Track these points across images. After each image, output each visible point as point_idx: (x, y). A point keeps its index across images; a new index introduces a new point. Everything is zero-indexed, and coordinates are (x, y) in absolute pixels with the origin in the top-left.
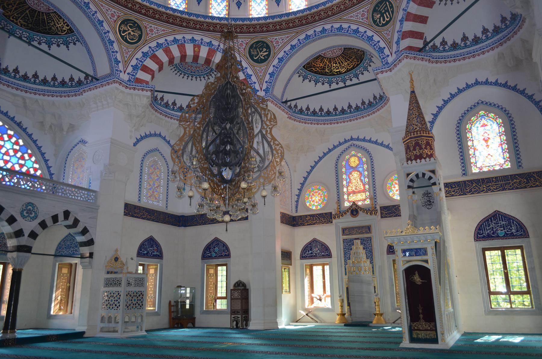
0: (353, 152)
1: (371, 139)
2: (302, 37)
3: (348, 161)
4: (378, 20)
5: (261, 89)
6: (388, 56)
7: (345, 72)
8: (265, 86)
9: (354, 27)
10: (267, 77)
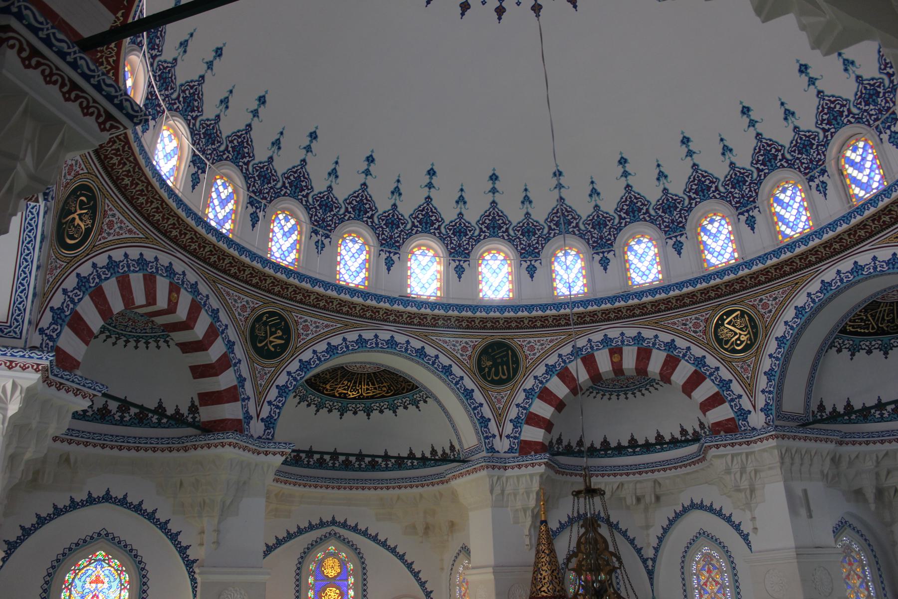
0: (332, 548)
1: (367, 529)
3: (320, 564)
4: (487, 370)
5: (258, 416)
6: (494, 436)
7: (354, 398)
8: (265, 412)
9: (445, 360)
10: (273, 394)
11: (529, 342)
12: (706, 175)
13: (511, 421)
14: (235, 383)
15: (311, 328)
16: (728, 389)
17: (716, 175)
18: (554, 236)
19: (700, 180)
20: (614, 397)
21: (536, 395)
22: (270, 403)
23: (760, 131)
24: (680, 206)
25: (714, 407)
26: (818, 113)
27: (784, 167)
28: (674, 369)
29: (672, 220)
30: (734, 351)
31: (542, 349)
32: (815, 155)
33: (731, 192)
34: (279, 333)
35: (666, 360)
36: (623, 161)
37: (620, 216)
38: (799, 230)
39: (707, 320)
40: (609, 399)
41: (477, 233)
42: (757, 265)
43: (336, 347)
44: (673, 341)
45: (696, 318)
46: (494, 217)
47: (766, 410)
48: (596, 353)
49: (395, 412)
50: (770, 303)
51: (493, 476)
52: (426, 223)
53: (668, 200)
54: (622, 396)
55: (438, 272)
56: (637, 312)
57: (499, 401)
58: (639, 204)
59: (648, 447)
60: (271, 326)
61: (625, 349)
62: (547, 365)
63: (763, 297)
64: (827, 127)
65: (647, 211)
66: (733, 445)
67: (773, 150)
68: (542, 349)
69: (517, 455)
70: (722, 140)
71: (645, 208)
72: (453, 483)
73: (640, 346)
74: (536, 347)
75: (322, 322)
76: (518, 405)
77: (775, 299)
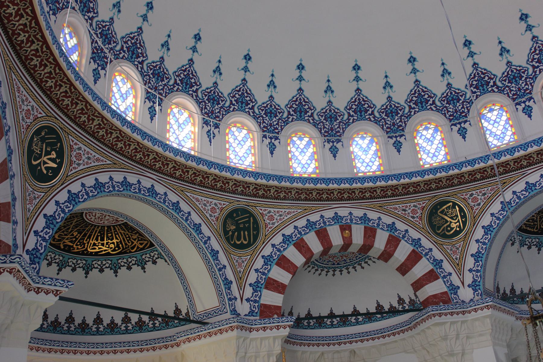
2: (118, 177)
4: (230, 233)
5: (24, 246)
6: (236, 299)
9: (196, 219)
10: (40, 224)
11: (270, 212)
12: (426, 90)
13: (250, 285)
14: (9, 200)
15: (84, 158)
16: (441, 267)
17: (434, 92)
18: (292, 121)
19: (419, 94)
20: (324, 273)
21: (275, 262)
22: (36, 233)
23: (476, 62)
24: (401, 113)
25: (431, 282)
26: (530, 53)
27: (494, 92)
28: (396, 247)
29: (393, 123)
30: (444, 236)
31: (280, 219)
32: (523, 85)
33: (446, 107)
34: (54, 155)
35: (388, 239)
36: (356, 67)
37: (349, 113)
38: (505, 142)
39: (423, 208)
40: (320, 274)
41: (228, 104)
42: (479, 163)
43: (103, 185)
44: (394, 223)
45: (414, 206)
46: (243, 93)
47: (474, 286)
48: (328, 228)
49: (116, 272)
50: (479, 197)
51: (240, 337)
52: (187, 84)
53: (391, 106)
54: (331, 272)
55: (192, 132)
56: (367, 195)
57: (240, 265)
58: (366, 106)
59: (344, 320)
60: (48, 145)
61: (354, 227)
62: (283, 235)
63: (474, 192)
64: (536, 65)
65: (373, 113)
66: (452, 314)
67: (486, 78)
68: (280, 219)
69: (258, 318)
70: (443, 64)
71: (371, 110)
72: (183, 346)
73: (366, 225)
74: (276, 217)
75: (94, 154)
76: (257, 270)
77: (484, 194)
